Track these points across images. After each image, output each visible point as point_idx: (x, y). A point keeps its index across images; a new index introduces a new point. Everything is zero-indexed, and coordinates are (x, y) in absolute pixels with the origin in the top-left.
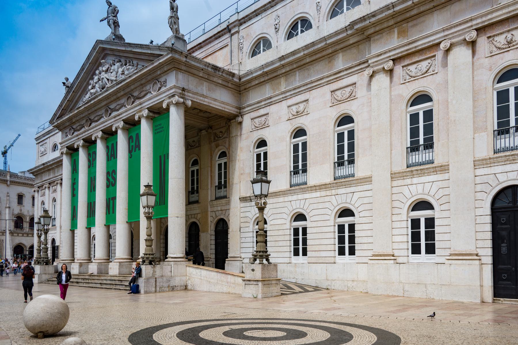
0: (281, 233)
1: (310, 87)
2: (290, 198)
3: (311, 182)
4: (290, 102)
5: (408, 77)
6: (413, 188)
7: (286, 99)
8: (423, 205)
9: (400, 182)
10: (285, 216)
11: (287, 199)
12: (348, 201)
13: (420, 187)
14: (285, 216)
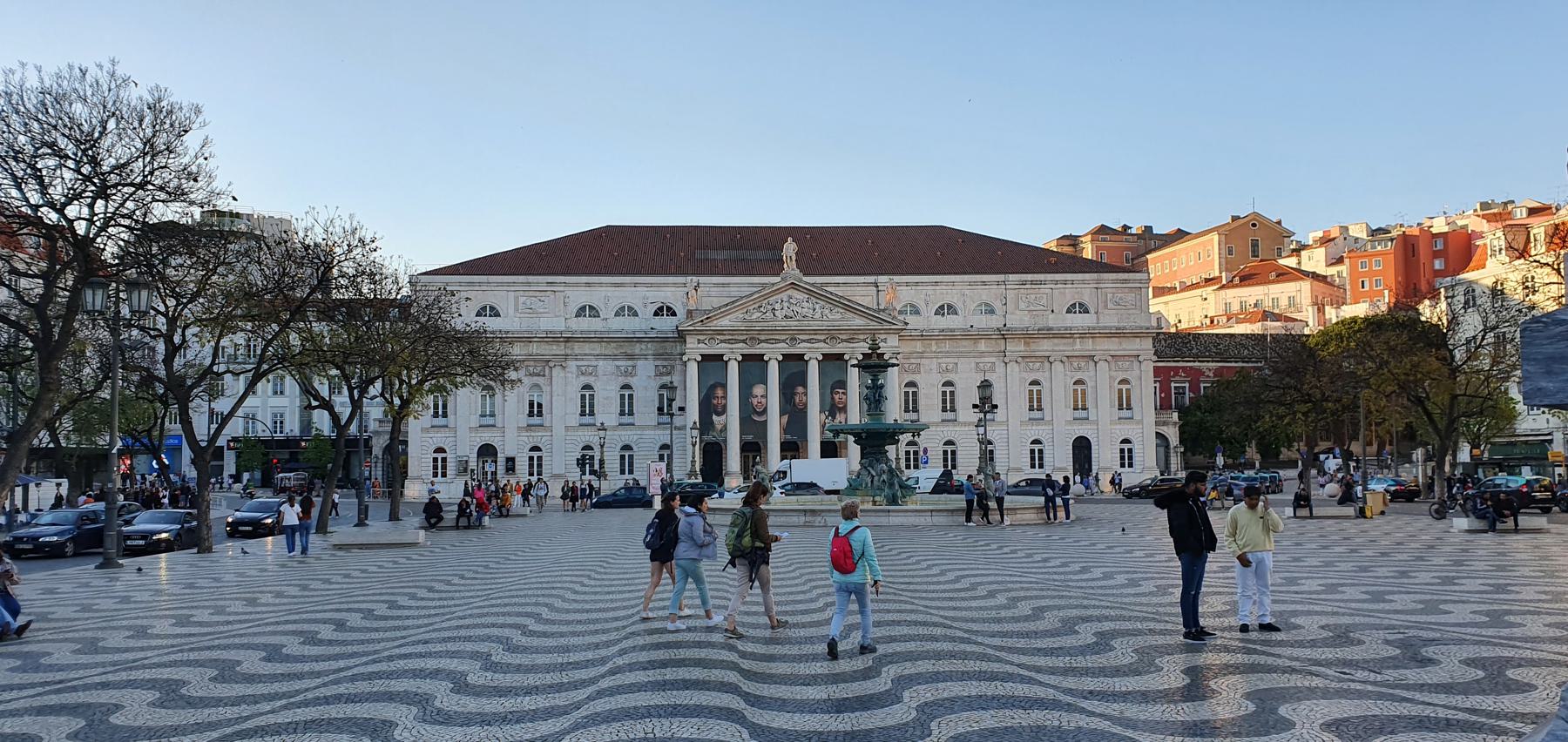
1: (961, 355)
3: (960, 419)
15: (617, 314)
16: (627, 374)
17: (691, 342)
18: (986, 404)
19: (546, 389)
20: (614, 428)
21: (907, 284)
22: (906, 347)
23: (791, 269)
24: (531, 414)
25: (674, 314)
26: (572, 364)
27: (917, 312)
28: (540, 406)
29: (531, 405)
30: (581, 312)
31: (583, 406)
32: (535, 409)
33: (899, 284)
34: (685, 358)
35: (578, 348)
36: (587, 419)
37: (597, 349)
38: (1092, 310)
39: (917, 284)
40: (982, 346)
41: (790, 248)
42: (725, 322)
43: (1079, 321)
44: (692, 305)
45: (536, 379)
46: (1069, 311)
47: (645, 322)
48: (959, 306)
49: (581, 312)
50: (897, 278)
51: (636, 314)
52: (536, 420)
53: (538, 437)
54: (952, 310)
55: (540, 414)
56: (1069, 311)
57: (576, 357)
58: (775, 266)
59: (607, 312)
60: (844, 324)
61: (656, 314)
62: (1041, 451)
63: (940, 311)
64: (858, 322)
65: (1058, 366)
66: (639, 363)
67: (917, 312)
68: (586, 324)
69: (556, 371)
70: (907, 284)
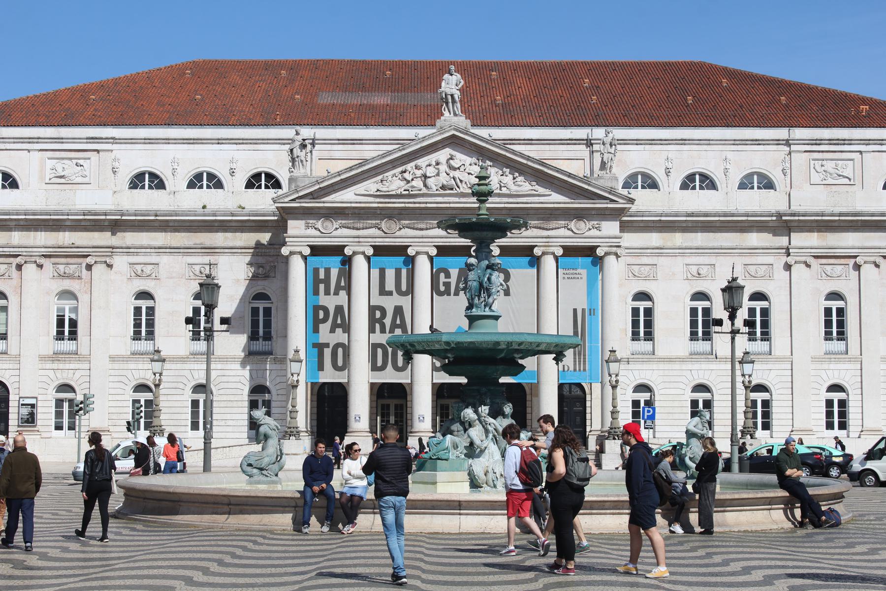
0: (676, 404)
4: (689, 260)
5: (824, 275)
6: (830, 373)
7: (683, 255)
8: (836, 388)
9: (819, 366)
10: (682, 386)
11: (684, 366)
12: (764, 377)
13: (836, 372)
14: (683, 386)
15: (191, 185)
17: (295, 227)
18: (760, 326)
19: (84, 298)
20: (182, 360)
21: (638, 142)
22: (631, 239)
23: (453, 120)
24: (60, 336)
25: (277, 185)
26: (120, 262)
27: (654, 185)
28: (73, 323)
29: (60, 322)
30: (137, 181)
31: (137, 325)
32: (67, 329)
33: (625, 142)
34: (285, 251)
36: (144, 345)
39: (651, 142)
40: (754, 239)
41: (451, 84)
42: (347, 197)
44: (297, 173)
45: (67, 284)
47: (234, 199)
48: (717, 176)
49: (137, 181)
50: (619, 133)
51: (219, 185)
52: (67, 345)
53: (69, 373)
54: (708, 182)
55: (73, 335)
57: (128, 250)
58: (430, 117)
59: (177, 182)
60: (534, 202)
61: (250, 185)
62: (843, 403)
63: (688, 183)
64: (556, 199)
65: (868, 270)
66: (223, 261)
67: (652, 184)
69: (99, 270)
70: (638, 142)
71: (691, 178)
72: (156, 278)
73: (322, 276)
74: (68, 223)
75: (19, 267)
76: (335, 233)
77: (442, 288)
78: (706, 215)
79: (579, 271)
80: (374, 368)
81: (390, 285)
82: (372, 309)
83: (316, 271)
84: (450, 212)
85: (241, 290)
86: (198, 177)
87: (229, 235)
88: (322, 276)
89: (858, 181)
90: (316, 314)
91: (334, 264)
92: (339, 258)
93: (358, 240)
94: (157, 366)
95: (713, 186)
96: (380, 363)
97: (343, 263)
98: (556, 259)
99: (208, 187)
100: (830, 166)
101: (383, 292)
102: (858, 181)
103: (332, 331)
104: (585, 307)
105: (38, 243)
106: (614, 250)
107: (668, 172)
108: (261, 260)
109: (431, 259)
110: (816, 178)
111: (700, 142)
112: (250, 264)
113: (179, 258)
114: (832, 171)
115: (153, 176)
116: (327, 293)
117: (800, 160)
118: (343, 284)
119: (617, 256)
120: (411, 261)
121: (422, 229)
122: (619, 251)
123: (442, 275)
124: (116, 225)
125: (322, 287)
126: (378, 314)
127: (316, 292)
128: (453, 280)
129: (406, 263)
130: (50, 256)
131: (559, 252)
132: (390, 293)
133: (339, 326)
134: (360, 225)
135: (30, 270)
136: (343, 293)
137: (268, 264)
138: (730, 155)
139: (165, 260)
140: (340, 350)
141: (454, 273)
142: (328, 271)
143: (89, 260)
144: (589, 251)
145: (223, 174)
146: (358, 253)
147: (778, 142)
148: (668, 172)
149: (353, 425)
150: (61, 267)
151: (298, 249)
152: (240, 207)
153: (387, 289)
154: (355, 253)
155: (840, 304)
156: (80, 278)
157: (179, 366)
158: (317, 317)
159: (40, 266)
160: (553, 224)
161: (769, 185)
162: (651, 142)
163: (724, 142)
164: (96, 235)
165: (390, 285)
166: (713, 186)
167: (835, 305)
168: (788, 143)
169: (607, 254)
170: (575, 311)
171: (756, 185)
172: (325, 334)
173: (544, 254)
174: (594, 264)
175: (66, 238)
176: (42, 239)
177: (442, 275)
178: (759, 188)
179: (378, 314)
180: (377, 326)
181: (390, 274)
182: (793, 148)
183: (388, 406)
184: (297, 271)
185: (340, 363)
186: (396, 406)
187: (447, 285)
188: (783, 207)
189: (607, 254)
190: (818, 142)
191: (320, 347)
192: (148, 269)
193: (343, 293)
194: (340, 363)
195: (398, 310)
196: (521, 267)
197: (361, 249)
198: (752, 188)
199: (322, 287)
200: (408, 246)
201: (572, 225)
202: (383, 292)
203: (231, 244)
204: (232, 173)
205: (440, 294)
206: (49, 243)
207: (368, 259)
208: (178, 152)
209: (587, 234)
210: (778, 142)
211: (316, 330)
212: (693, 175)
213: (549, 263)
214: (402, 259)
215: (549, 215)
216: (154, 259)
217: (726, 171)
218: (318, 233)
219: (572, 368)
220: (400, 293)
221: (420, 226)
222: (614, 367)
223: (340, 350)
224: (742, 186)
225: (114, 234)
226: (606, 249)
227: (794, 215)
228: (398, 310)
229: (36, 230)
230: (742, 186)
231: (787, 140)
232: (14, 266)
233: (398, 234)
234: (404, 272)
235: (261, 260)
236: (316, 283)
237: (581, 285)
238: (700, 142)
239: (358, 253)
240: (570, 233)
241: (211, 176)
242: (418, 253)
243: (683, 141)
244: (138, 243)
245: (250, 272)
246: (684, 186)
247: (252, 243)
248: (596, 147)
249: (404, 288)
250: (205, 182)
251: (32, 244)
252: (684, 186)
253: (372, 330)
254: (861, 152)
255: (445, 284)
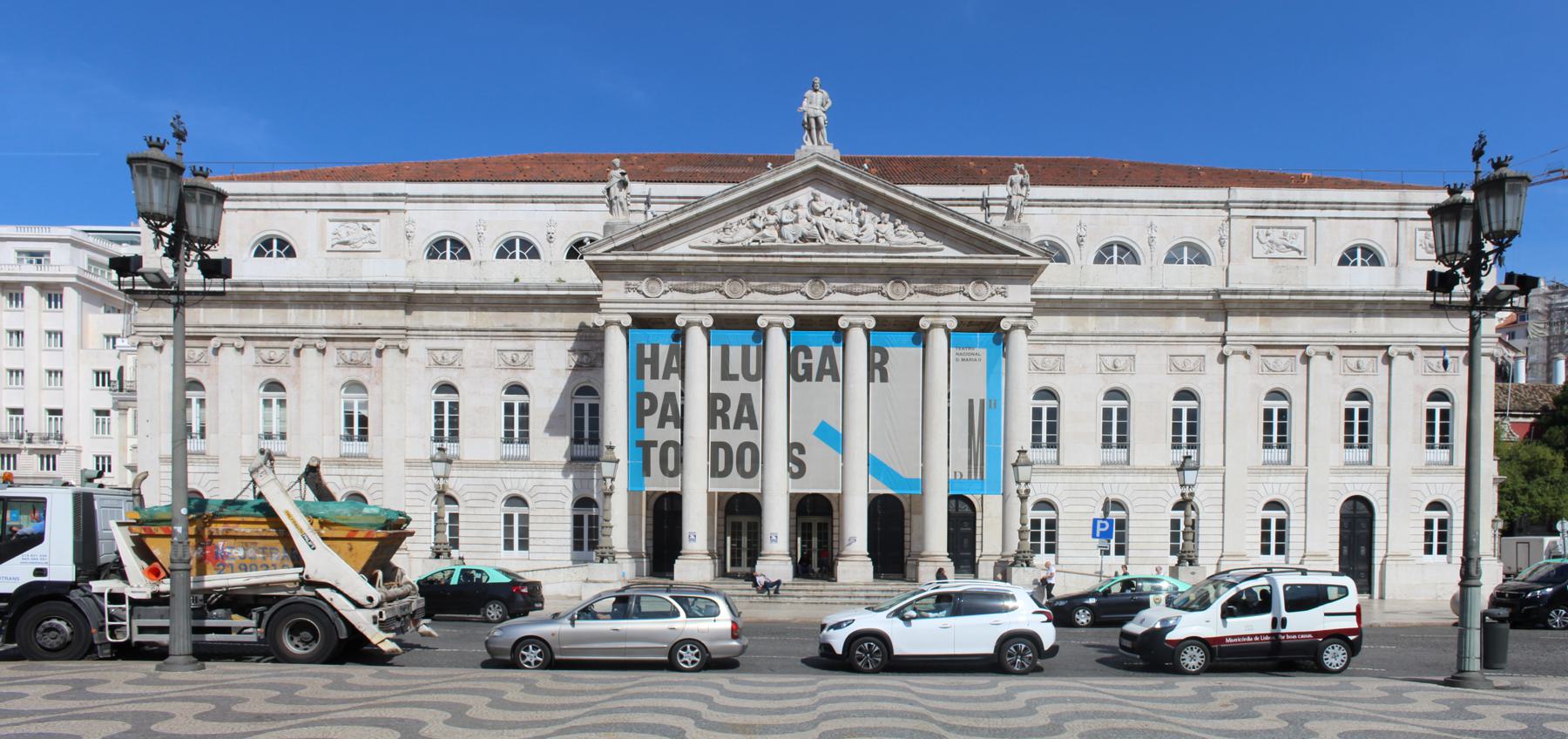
2: (1101, 479)
15: (501, 254)
16: (514, 365)
26: (417, 346)
35: (427, 318)
37: (464, 319)
38: (1388, 258)
39: (1061, 203)
43: (1362, 279)
45: (354, 374)
46: (1343, 262)
48: (1140, 246)
51: (535, 254)
54: (1128, 254)
56: (1343, 262)
57: (425, 333)
63: (1104, 255)
66: (540, 346)
67: (1062, 258)
68: (448, 272)
71: (1107, 249)
72: (460, 368)
73: (648, 354)
74: (352, 298)
75: (297, 352)
76: (664, 298)
77: (801, 372)
78: (1128, 292)
79: (977, 350)
80: (714, 472)
81: (735, 366)
82: (712, 398)
83: (641, 348)
84: (811, 270)
85: (561, 382)
86: (510, 244)
87: (547, 315)
88: (648, 354)
89: (1310, 255)
90: (640, 404)
91: (663, 340)
92: (670, 332)
93: (694, 307)
94: (440, 468)
95: (1135, 259)
96: (721, 467)
97: (676, 338)
98: (948, 332)
99: (522, 256)
100: (1276, 235)
101: (726, 376)
102: (1310, 255)
103: (661, 425)
104: (984, 397)
105: (319, 324)
106: (1023, 322)
107: (1080, 241)
108: (585, 346)
109: (787, 332)
110: (1259, 250)
111: (1121, 204)
112: (573, 351)
113: (487, 343)
114: (1279, 241)
115: (456, 243)
116: (654, 376)
117: (1241, 227)
118: (674, 365)
119: (1028, 331)
120: (761, 335)
121: (775, 293)
122: (1029, 324)
123: (801, 355)
124: (410, 301)
125: (648, 368)
126: (720, 404)
127: (640, 376)
128: (815, 362)
129: (756, 339)
130: (333, 339)
131: (953, 324)
132: (735, 377)
133: (669, 419)
134: (695, 287)
135: (309, 354)
136: (675, 377)
137: (589, 348)
138: (1156, 221)
139: (470, 345)
140: (671, 451)
141: (817, 352)
142: (655, 348)
143: (379, 344)
144: (989, 326)
145: (539, 241)
146: (694, 324)
147: (1215, 205)
148: (1080, 241)
149: (688, 545)
150: (347, 353)
151: (615, 318)
152: (560, 281)
153: (731, 372)
154: (689, 324)
155: (1283, 404)
156: (369, 366)
157: (488, 473)
158: (641, 406)
159: (323, 351)
160: (945, 288)
161: (1201, 257)
162: (1061, 203)
163: (1149, 204)
164: (387, 313)
165: (735, 366)
166: (1135, 259)
167: (1276, 405)
168: (1227, 206)
169: (1014, 327)
170: (971, 401)
171: (1186, 258)
172: (652, 429)
173: (932, 326)
174: (997, 341)
175: (351, 317)
176: (323, 318)
177: (801, 355)
178: (1190, 262)
179: (720, 404)
180: (719, 419)
181: (736, 353)
182: (1234, 212)
183: (740, 525)
184: (616, 348)
185: (671, 466)
186: (750, 525)
187: (808, 367)
188: (1221, 286)
189: (1014, 327)
190: (1263, 205)
191: (646, 446)
192: (450, 356)
193: (675, 377)
194: (671, 466)
195: (746, 399)
196: (901, 345)
197: (697, 318)
198: (1181, 262)
199: (648, 368)
200: (757, 316)
201: (970, 289)
202: (726, 376)
203: (549, 327)
204: (550, 239)
205: (799, 379)
206: (331, 324)
207: (707, 331)
208: (483, 215)
209: (989, 301)
210: (1215, 205)
211: (640, 424)
212: (1110, 245)
213: (938, 339)
214: (751, 333)
215: (939, 275)
216: (456, 344)
217: (1151, 239)
218: (641, 297)
219: (965, 476)
220: (748, 377)
221: (773, 289)
222: (1024, 472)
223: (671, 451)
224: (1169, 260)
225: (408, 312)
226: (1014, 321)
227: (1235, 292)
228: (746, 399)
229: (316, 307)
230: (1169, 260)
231: (1227, 203)
232: (292, 351)
233: (745, 299)
234: (753, 350)
235: (585, 346)
236: (640, 364)
237: (980, 367)
238: (1121, 204)
239: (694, 324)
240: (967, 300)
241: (525, 244)
242: (770, 324)
243: (1100, 203)
244: (437, 325)
245: (573, 360)
246: (1099, 260)
247: (576, 326)
248: (993, 209)
249: (753, 371)
250: (518, 251)
251: (311, 324)
252: (1099, 260)
253: (712, 425)
254: (1314, 219)
255: (805, 366)
